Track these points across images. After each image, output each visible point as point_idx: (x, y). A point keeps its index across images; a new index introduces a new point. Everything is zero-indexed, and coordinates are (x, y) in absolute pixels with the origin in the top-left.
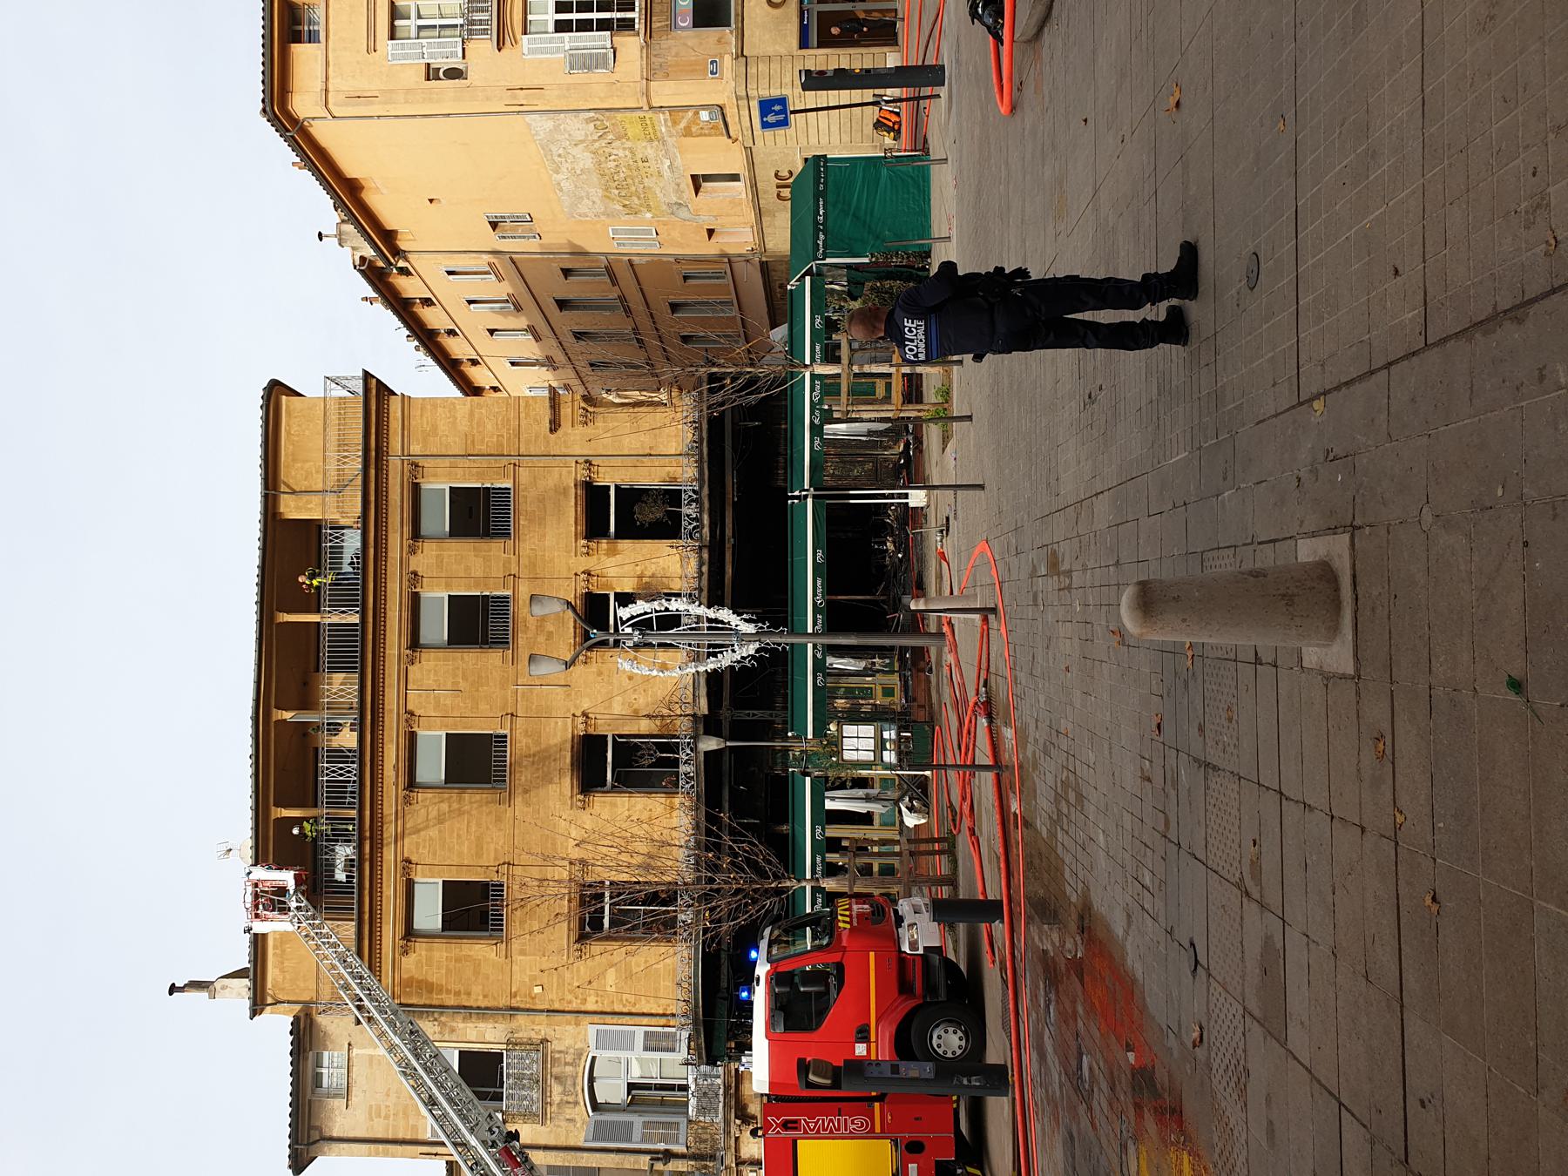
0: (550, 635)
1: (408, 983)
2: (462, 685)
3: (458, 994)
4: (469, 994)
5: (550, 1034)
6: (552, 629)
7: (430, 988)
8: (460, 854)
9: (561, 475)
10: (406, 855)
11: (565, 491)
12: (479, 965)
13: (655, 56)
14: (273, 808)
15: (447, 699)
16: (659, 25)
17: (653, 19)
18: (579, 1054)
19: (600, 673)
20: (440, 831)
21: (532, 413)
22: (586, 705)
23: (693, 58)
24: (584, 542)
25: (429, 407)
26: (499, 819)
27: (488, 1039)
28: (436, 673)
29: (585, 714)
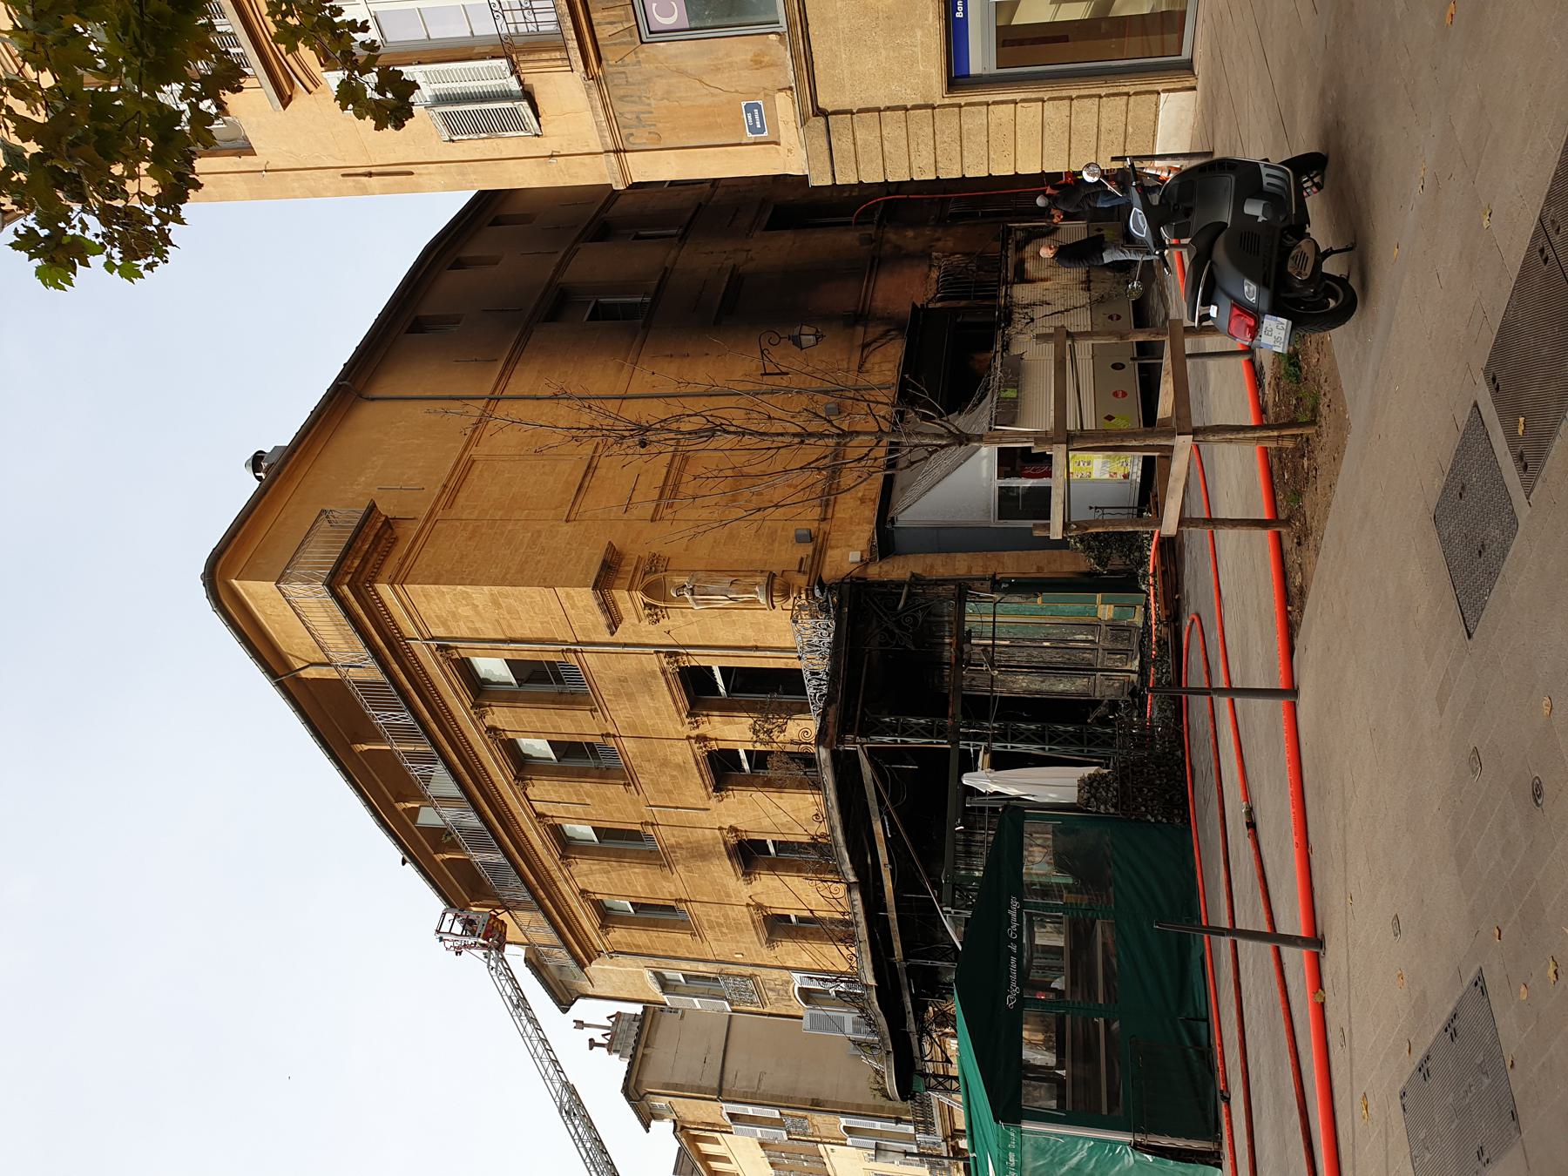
0: (673, 777)
2: (588, 801)
5: (756, 973)
6: (675, 773)
7: (638, 947)
8: (637, 892)
9: (641, 661)
10: (580, 886)
11: (653, 674)
13: (621, 98)
14: (435, 856)
15: (579, 809)
16: (611, 30)
17: (595, 16)
18: (788, 982)
19: (741, 803)
20: (608, 878)
21: (580, 604)
22: (733, 822)
23: (707, 101)
24: (687, 720)
25: (433, 594)
26: (665, 878)
27: (701, 969)
28: (555, 792)
29: (733, 829)
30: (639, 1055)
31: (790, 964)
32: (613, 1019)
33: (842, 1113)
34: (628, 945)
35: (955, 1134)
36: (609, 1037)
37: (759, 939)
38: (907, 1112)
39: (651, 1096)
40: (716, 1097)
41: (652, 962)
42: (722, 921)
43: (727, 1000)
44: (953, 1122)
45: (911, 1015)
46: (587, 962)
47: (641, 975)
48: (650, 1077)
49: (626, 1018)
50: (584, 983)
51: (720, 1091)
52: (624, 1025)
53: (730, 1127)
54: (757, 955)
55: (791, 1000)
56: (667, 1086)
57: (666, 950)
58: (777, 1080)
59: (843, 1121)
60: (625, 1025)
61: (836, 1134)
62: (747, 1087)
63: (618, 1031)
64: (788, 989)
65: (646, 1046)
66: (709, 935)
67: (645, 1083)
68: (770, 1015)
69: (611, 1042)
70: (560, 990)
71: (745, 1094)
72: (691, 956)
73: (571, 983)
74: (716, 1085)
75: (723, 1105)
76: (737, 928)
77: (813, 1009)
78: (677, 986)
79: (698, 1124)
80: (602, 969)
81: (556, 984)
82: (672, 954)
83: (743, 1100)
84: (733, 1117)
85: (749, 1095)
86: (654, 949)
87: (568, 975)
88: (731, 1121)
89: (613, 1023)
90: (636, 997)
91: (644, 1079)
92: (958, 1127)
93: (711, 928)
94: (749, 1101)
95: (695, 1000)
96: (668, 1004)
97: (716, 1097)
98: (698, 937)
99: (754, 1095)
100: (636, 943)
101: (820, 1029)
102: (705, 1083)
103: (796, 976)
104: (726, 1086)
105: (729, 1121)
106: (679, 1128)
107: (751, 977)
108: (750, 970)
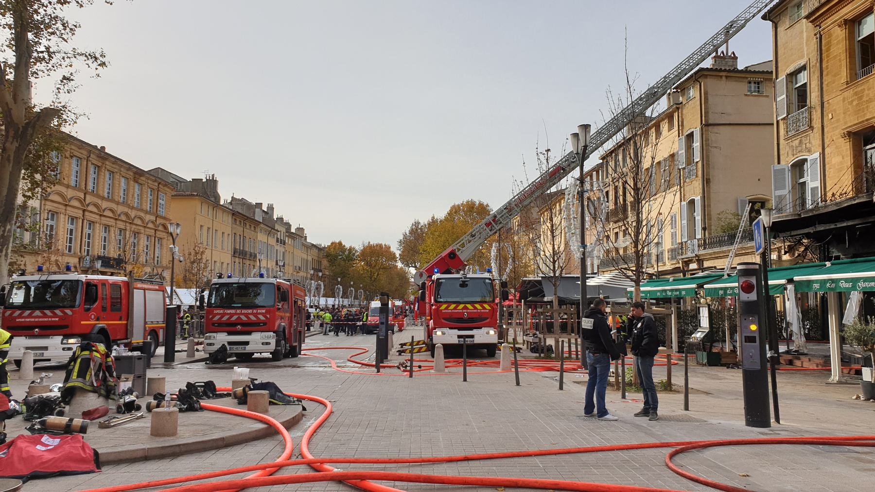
1: (830, 36)
3: (827, 68)
4: (827, 75)
7: (828, 50)
12: (839, 75)
27: (812, 94)
30: (721, 74)
31: (827, 151)
32: (732, 55)
33: (704, 196)
34: (829, 43)
35: (700, 261)
36: (722, 55)
37: (850, 127)
38: (710, 234)
39: (699, 87)
40: (704, 122)
41: (814, 60)
42: (865, 99)
43: (787, 116)
44: (708, 260)
45: (833, 226)
46: (811, 19)
47: (802, 57)
48: (710, 83)
49: (734, 63)
50: (787, 23)
51: (707, 125)
52: (730, 62)
53: (682, 135)
54: (833, 128)
55: (793, 155)
56: (706, 93)
57: (827, 68)
58: (717, 157)
59: (698, 199)
60: (731, 63)
61: (687, 196)
62: (712, 140)
63: (727, 60)
64: (803, 152)
65: (727, 77)
66: (849, 93)
67: (706, 80)
68: (778, 145)
69: (719, 57)
70: (782, 8)
71: (707, 140)
72: (824, 86)
73: (786, 15)
74: (710, 122)
75: (698, 129)
76: (859, 110)
77: (789, 170)
78: (792, 82)
79: (682, 117)
80: (802, 32)
81: (784, 6)
82: (825, 73)
83: (704, 139)
84: (690, 136)
85: (707, 142)
86: (828, 61)
87: (792, 12)
88: (687, 135)
89: (731, 56)
90: (779, 59)
91: (708, 80)
92: (705, 262)
93: (856, 94)
94: (704, 143)
95: (784, 96)
96: (778, 80)
97: (704, 122)
98: (846, 86)
99: (708, 145)
100: (832, 47)
101: (775, 176)
102: (711, 115)
103: (817, 155)
104: (710, 128)
105: (687, 134)
106: (678, 106)
107: (811, 127)
108: (817, 124)
